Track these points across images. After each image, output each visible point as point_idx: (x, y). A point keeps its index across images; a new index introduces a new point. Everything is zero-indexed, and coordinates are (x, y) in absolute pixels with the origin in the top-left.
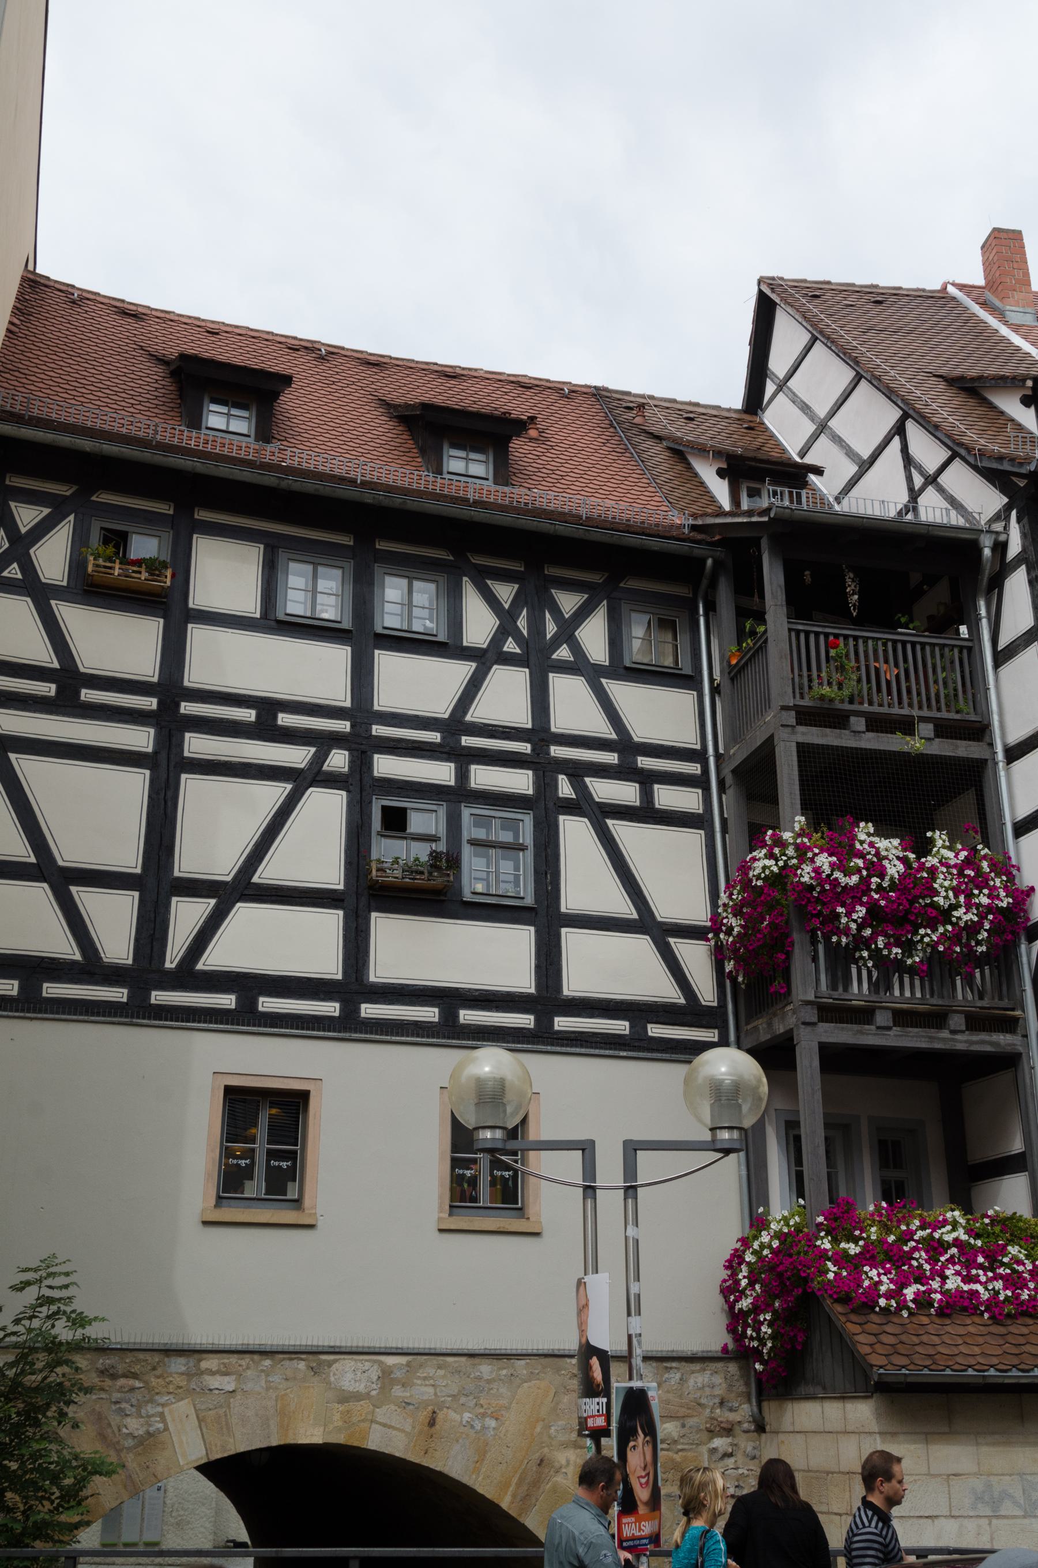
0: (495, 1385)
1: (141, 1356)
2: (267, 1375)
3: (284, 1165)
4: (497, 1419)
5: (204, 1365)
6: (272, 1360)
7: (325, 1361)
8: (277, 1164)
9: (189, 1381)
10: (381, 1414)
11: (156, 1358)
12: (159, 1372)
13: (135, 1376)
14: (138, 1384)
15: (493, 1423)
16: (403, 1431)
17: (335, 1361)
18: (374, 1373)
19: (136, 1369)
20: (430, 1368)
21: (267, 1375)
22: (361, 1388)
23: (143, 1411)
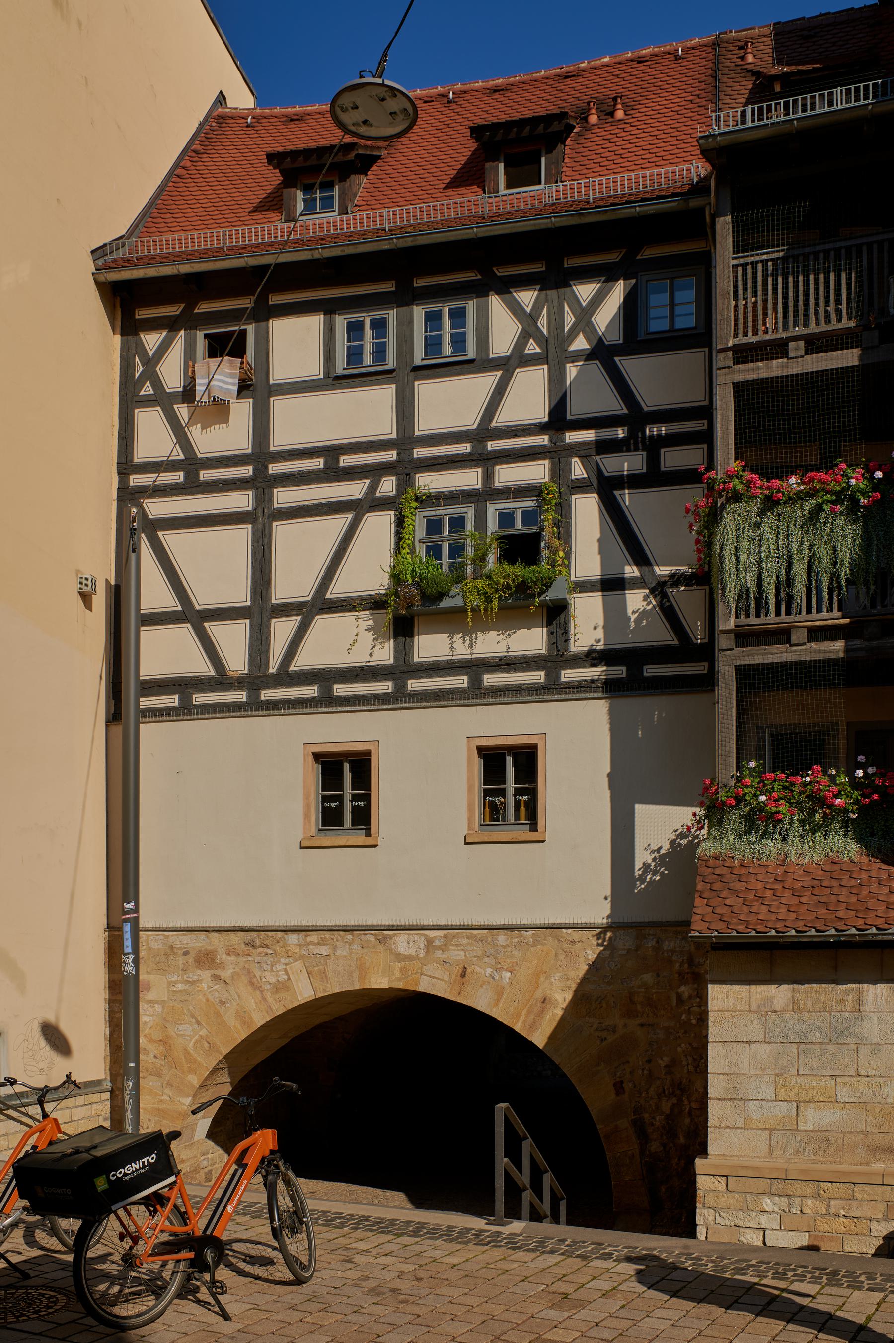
0: (509, 950)
1: (270, 934)
2: (350, 945)
3: (333, 805)
4: (511, 972)
5: (309, 939)
6: (353, 935)
7: (388, 935)
8: (328, 805)
9: (300, 949)
10: (428, 969)
11: (280, 934)
12: (281, 944)
13: (267, 947)
14: (269, 951)
15: (508, 975)
16: (442, 980)
17: (395, 935)
18: (422, 943)
19: (267, 942)
20: (463, 938)
21: (350, 945)
22: (412, 952)
23: (274, 969)
